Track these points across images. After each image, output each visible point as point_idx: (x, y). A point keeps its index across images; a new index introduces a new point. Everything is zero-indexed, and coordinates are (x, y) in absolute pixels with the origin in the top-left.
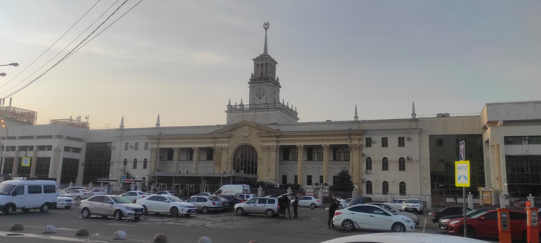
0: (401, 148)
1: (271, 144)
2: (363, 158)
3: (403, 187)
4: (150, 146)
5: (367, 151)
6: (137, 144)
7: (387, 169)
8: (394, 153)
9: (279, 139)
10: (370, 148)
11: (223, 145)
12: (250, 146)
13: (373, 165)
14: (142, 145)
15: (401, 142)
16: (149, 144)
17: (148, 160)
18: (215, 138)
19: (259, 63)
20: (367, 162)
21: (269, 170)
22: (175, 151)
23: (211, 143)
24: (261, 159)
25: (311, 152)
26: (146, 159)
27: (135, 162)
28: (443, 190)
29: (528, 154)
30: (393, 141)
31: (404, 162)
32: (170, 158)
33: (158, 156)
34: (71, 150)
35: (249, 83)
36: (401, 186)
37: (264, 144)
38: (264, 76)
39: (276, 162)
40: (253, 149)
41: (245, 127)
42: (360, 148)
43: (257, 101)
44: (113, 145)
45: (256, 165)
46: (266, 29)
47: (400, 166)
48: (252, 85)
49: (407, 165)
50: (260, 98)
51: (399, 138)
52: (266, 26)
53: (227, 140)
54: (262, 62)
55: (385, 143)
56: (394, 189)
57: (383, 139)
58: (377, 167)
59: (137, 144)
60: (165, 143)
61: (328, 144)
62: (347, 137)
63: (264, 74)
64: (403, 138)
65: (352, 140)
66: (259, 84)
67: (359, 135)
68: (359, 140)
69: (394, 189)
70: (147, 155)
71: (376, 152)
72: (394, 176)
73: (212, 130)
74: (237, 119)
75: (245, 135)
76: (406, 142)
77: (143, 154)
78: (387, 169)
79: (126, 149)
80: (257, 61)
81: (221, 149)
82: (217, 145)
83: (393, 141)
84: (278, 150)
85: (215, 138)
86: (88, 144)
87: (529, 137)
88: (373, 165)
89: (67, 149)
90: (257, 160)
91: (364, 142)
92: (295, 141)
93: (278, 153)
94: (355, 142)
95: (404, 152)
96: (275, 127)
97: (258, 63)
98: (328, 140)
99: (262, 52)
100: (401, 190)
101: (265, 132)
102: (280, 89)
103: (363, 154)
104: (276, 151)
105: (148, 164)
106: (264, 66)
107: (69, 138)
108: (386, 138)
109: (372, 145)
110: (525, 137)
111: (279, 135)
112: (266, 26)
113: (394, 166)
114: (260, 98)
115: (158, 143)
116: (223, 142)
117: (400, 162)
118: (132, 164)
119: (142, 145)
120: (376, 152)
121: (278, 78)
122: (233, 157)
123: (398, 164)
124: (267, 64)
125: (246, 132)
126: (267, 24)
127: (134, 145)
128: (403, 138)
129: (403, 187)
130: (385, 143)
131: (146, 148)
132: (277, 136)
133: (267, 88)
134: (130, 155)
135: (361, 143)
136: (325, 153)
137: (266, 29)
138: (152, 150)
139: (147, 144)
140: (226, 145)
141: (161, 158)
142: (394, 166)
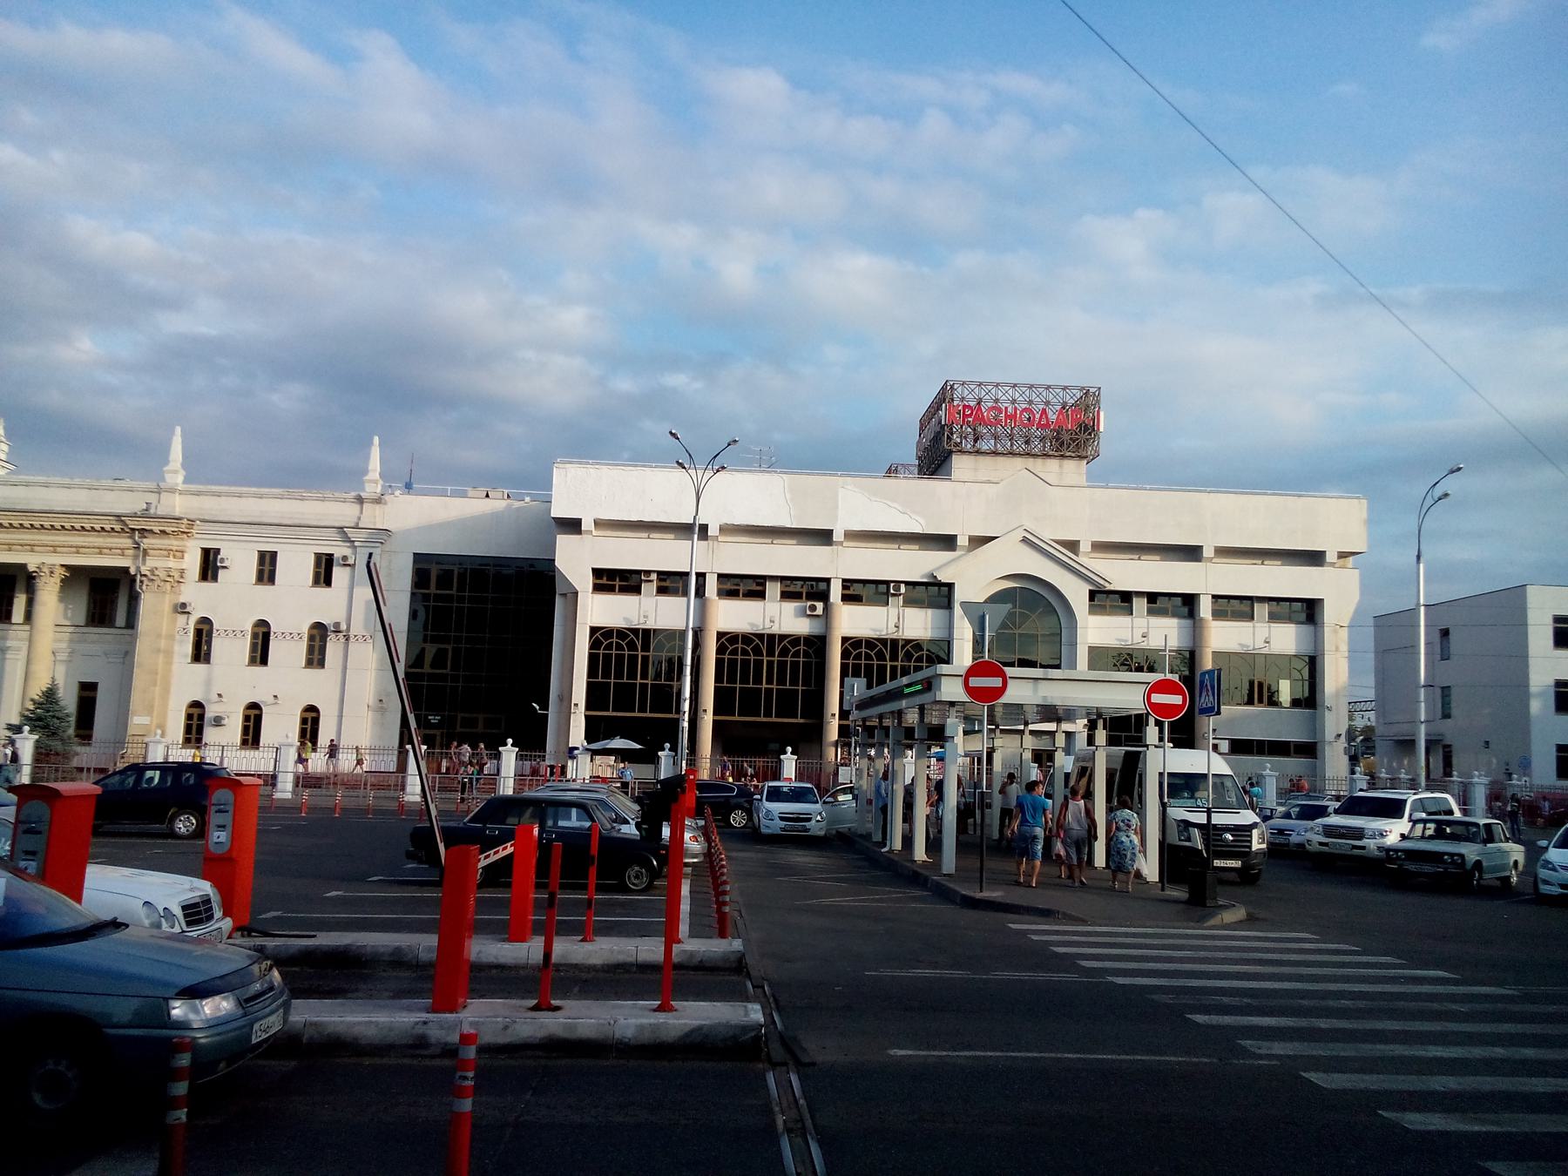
0: (323, 591)
2: (182, 619)
3: (310, 723)
5: (202, 599)
7: (264, 661)
8: (295, 604)
10: (213, 585)
13: (218, 646)
15: (324, 570)
20: (199, 633)
28: (438, 732)
30: (296, 564)
36: (304, 721)
47: (311, 650)
51: (318, 556)
55: (267, 569)
56: (281, 728)
57: (262, 555)
58: (231, 650)
62: (126, 542)
71: (234, 602)
76: (339, 574)
83: (296, 564)
87: (659, 573)
88: (217, 644)
91: (193, 562)
98: (54, 549)
103: (184, 605)
108: (274, 555)
109: (221, 572)
110: (648, 573)
113: (288, 652)
117: (311, 638)
120: (234, 602)
129: (310, 723)
130: (267, 569)
136: (49, 595)
142: (288, 652)
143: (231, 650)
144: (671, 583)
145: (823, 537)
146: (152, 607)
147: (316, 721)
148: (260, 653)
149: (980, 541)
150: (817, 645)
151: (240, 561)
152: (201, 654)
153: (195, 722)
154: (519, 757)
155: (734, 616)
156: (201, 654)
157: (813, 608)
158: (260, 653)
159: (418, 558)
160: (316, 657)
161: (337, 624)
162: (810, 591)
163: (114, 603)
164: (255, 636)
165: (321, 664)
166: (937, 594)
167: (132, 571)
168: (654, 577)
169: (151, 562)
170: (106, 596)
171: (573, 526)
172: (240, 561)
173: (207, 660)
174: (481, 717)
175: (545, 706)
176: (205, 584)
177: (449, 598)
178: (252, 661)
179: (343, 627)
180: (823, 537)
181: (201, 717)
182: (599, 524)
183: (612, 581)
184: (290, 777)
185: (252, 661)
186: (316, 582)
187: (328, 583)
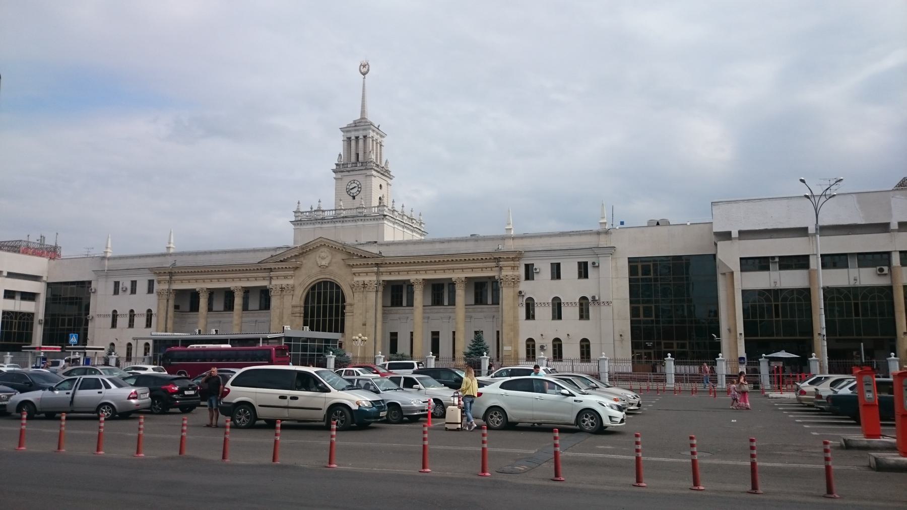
0: (583, 281)
1: (367, 279)
4: (156, 287)
6: (134, 283)
7: (560, 318)
8: (570, 288)
9: (381, 269)
10: (532, 282)
11: (284, 282)
12: (332, 283)
14: (142, 286)
15: (583, 271)
16: (156, 283)
17: (154, 311)
18: (271, 270)
19: (353, 135)
20: (528, 305)
21: (364, 325)
22: (201, 295)
23: (264, 278)
24: (351, 305)
25: (439, 292)
26: (149, 311)
27: (132, 314)
29: (778, 286)
30: (570, 269)
31: (588, 304)
32: (195, 307)
33: (172, 303)
35: (335, 171)
36: (582, 347)
37: (356, 279)
38: (361, 158)
39: (376, 310)
40: (338, 287)
41: (323, 249)
42: (515, 281)
43: (347, 202)
44: (93, 285)
45: (343, 314)
46: (364, 74)
47: (581, 310)
48: (339, 175)
49: (591, 309)
50: (354, 198)
51: (579, 263)
52: (364, 70)
53: (291, 273)
54: (357, 134)
56: (571, 351)
58: (543, 313)
59: (134, 283)
60: (182, 281)
61: (463, 275)
62: (494, 264)
64: (586, 264)
65: (501, 268)
66: (352, 173)
67: (513, 259)
68: (513, 268)
69: (571, 351)
70: (151, 302)
71: (542, 289)
72: (571, 328)
73: (267, 255)
74: (311, 234)
75: (323, 263)
77: (143, 302)
78: (560, 318)
79: (116, 292)
80: (347, 131)
81: (282, 289)
83: (570, 269)
84: (381, 289)
88: (537, 309)
90: (344, 308)
92: (408, 272)
93: (380, 294)
94: (507, 273)
95: (587, 288)
96: (374, 250)
97: (349, 135)
99: (358, 117)
100: (582, 353)
101: (354, 257)
103: (520, 292)
104: (377, 291)
105: (154, 319)
106: (361, 142)
107: (11, 275)
108: (558, 265)
111: (379, 263)
112: (364, 70)
113: (570, 312)
114: (354, 198)
115: (170, 282)
116: (286, 277)
117: (581, 304)
118: (127, 319)
119: (142, 286)
120: (542, 289)
122: (302, 303)
123: (577, 309)
124: (365, 137)
125: (323, 258)
126: (364, 66)
127: (128, 285)
128: (586, 264)
131: (150, 290)
132: (377, 265)
134: (124, 303)
135: (516, 273)
136: (460, 293)
137: (364, 74)
138: (159, 294)
139: (151, 283)
140: (290, 282)
141: (176, 307)
142: (570, 312)
143: (543, 313)
144: (865, 259)
145: (884, 227)
146: (507, 294)
147: (588, 346)
148: (557, 314)
150: (888, 291)
151: (544, 269)
152: (530, 315)
153: (531, 348)
154: (675, 364)
155: (839, 278)
156: (530, 315)
157: (881, 270)
158: (557, 314)
159: (631, 260)
160: (584, 314)
161: (594, 297)
162: (879, 260)
163: (442, 294)
164: (553, 305)
165: (588, 318)
167: (497, 277)
168: (777, 260)
169: (504, 273)
170: (484, 291)
171: (726, 236)
172: (544, 269)
173: (533, 318)
174: (675, 342)
175: (718, 336)
176: (528, 282)
177: (650, 279)
178: (554, 318)
179: (597, 298)
180: (884, 227)
181: (534, 346)
182: (740, 232)
183: (750, 264)
184: (607, 375)
185: (554, 318)
186: (580, 276)
187: (586, 276)
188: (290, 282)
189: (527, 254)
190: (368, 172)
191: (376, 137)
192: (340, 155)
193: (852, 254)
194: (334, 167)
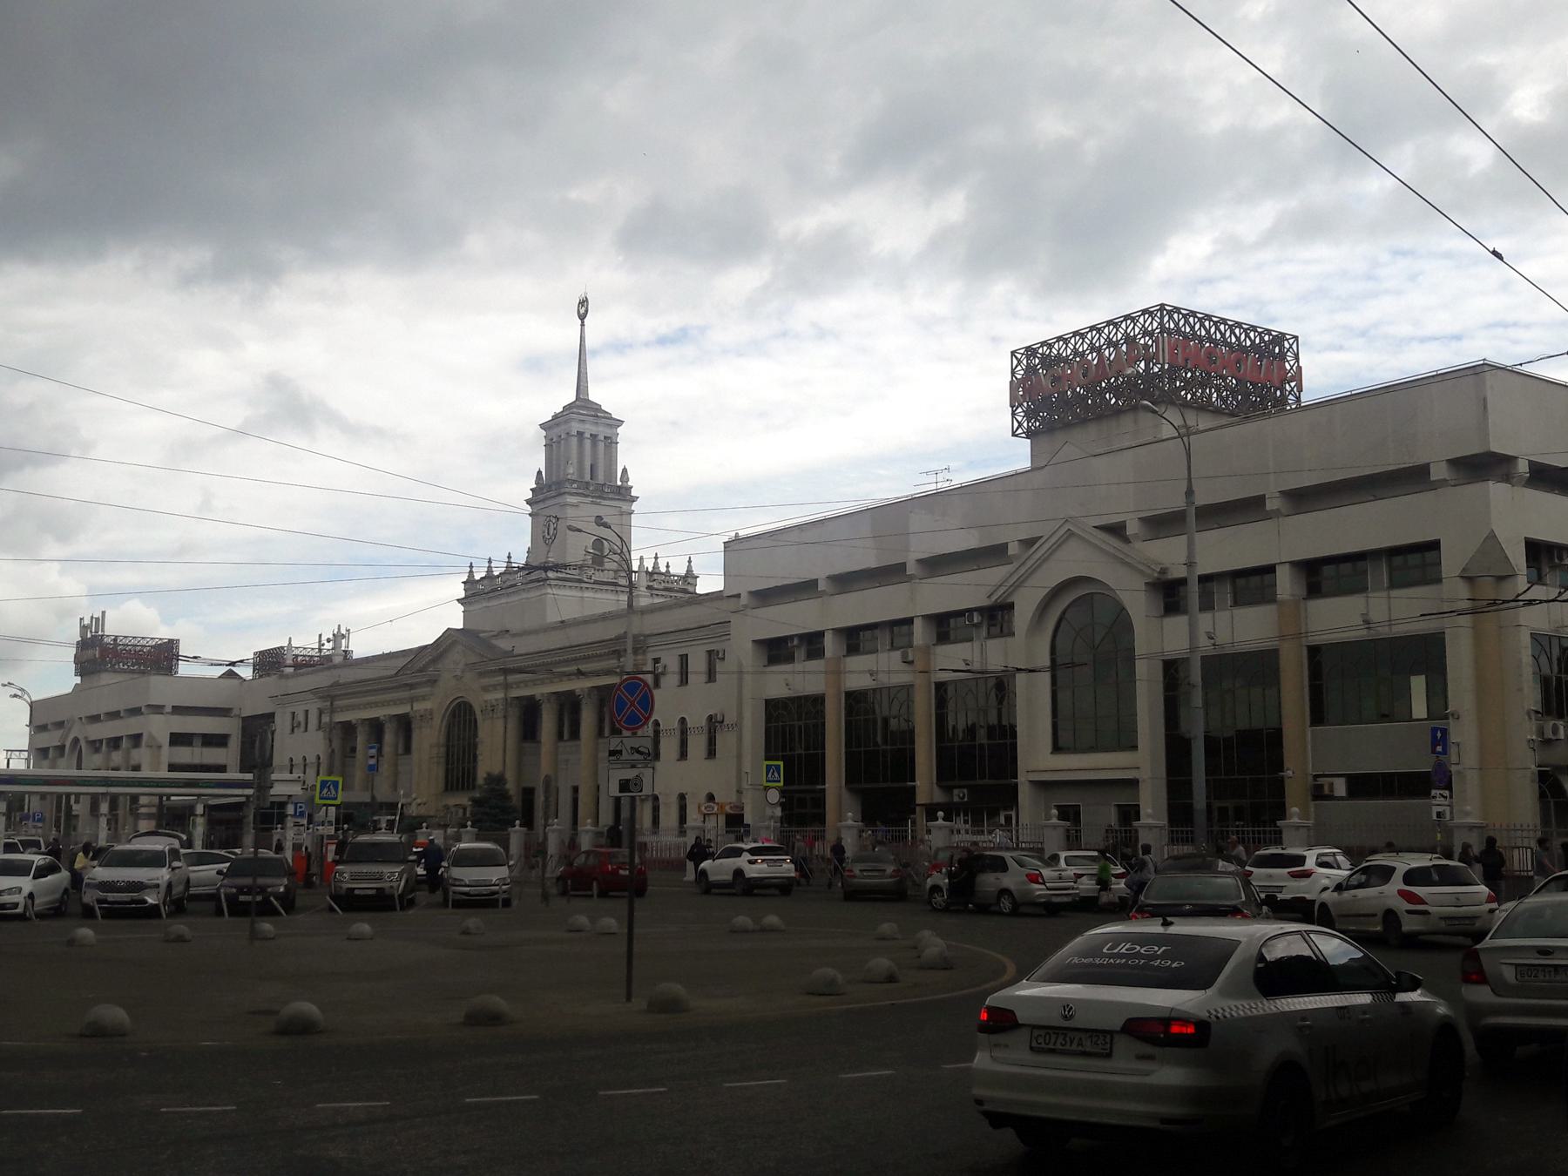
18: (411, 686)
19: (561, 430)
22: (360, 729)
23: (401, 702)
34: (198, 741)
35: (528, 502)
46: (582, 317)
63: (580, 463)
73: (401, 663)
82: (417, 706)
85: (411, 686)
86: (244, 719)
89: (178, 739)
102: (634, 506)
115: (333, 711)
121: (625, 470)
122: (442, 740)
133: (580, 511)
137: (582, 317)
149: (1029, 543)
166: (996, 616)
188: (427, 705)
189: (651, 641)
190: (559, 500)
191: (589, 429)
192: (539, 473)
193: (976, 609)
194: (530, 495)
